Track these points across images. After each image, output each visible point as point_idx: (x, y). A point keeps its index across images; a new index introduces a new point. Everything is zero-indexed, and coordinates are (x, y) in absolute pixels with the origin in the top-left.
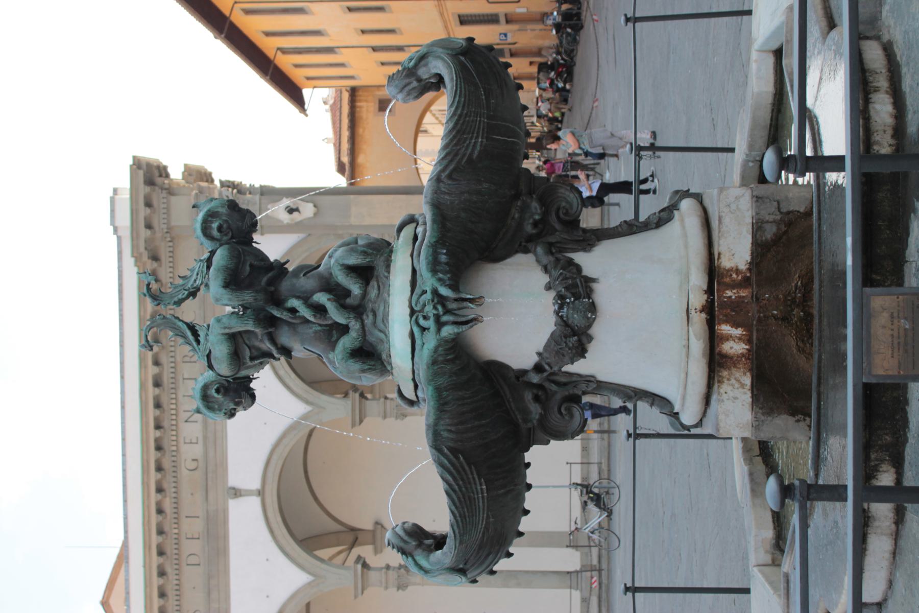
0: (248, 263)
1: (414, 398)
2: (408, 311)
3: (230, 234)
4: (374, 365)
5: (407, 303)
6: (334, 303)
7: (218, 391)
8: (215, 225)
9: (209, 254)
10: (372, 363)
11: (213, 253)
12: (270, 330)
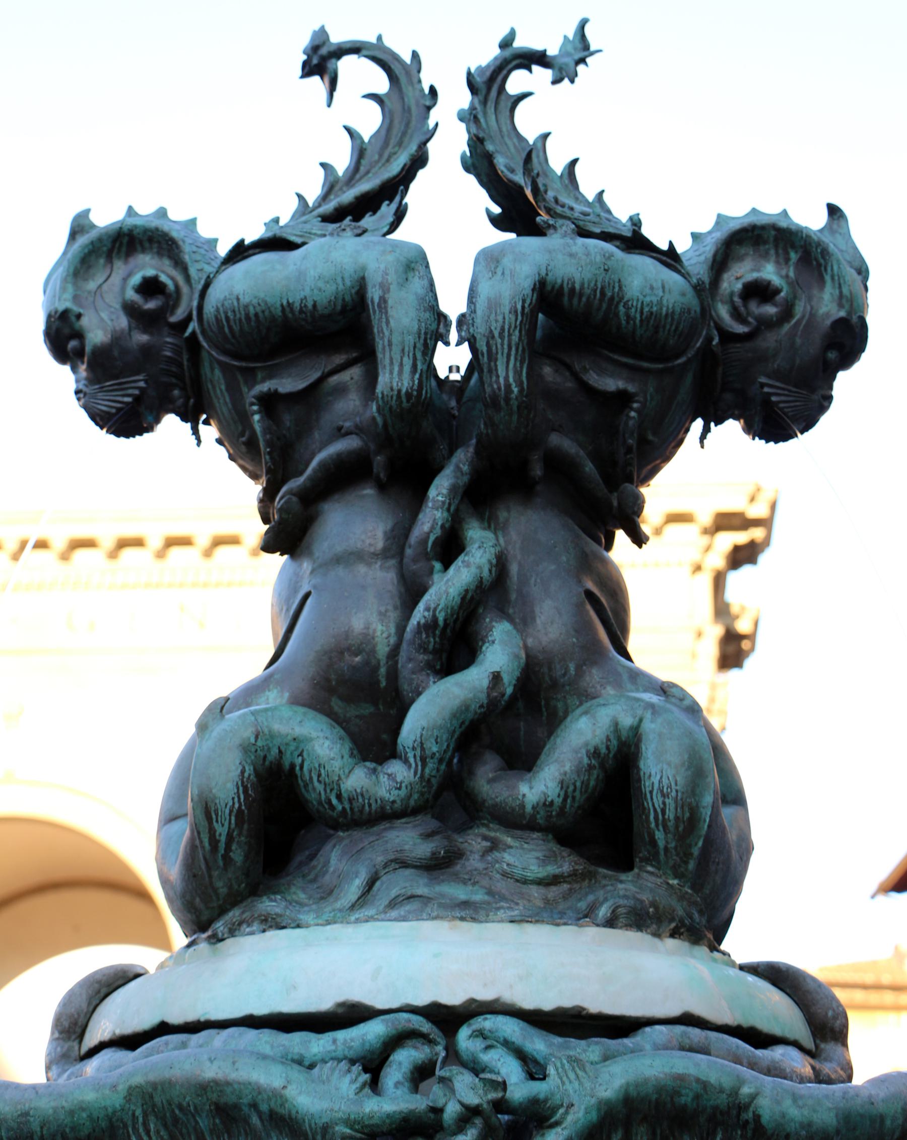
0: (631, 388)
1: (93, 1037)
2: (453, 997)
3: (740, 329)
4: (226, 858)
5: (485, 995)
6: (483, 698)
7: (150, 287)
8: (770, 272)
9: (664, 247)
10: (237, 855)
11: (670, 257)
12: (379, 460)
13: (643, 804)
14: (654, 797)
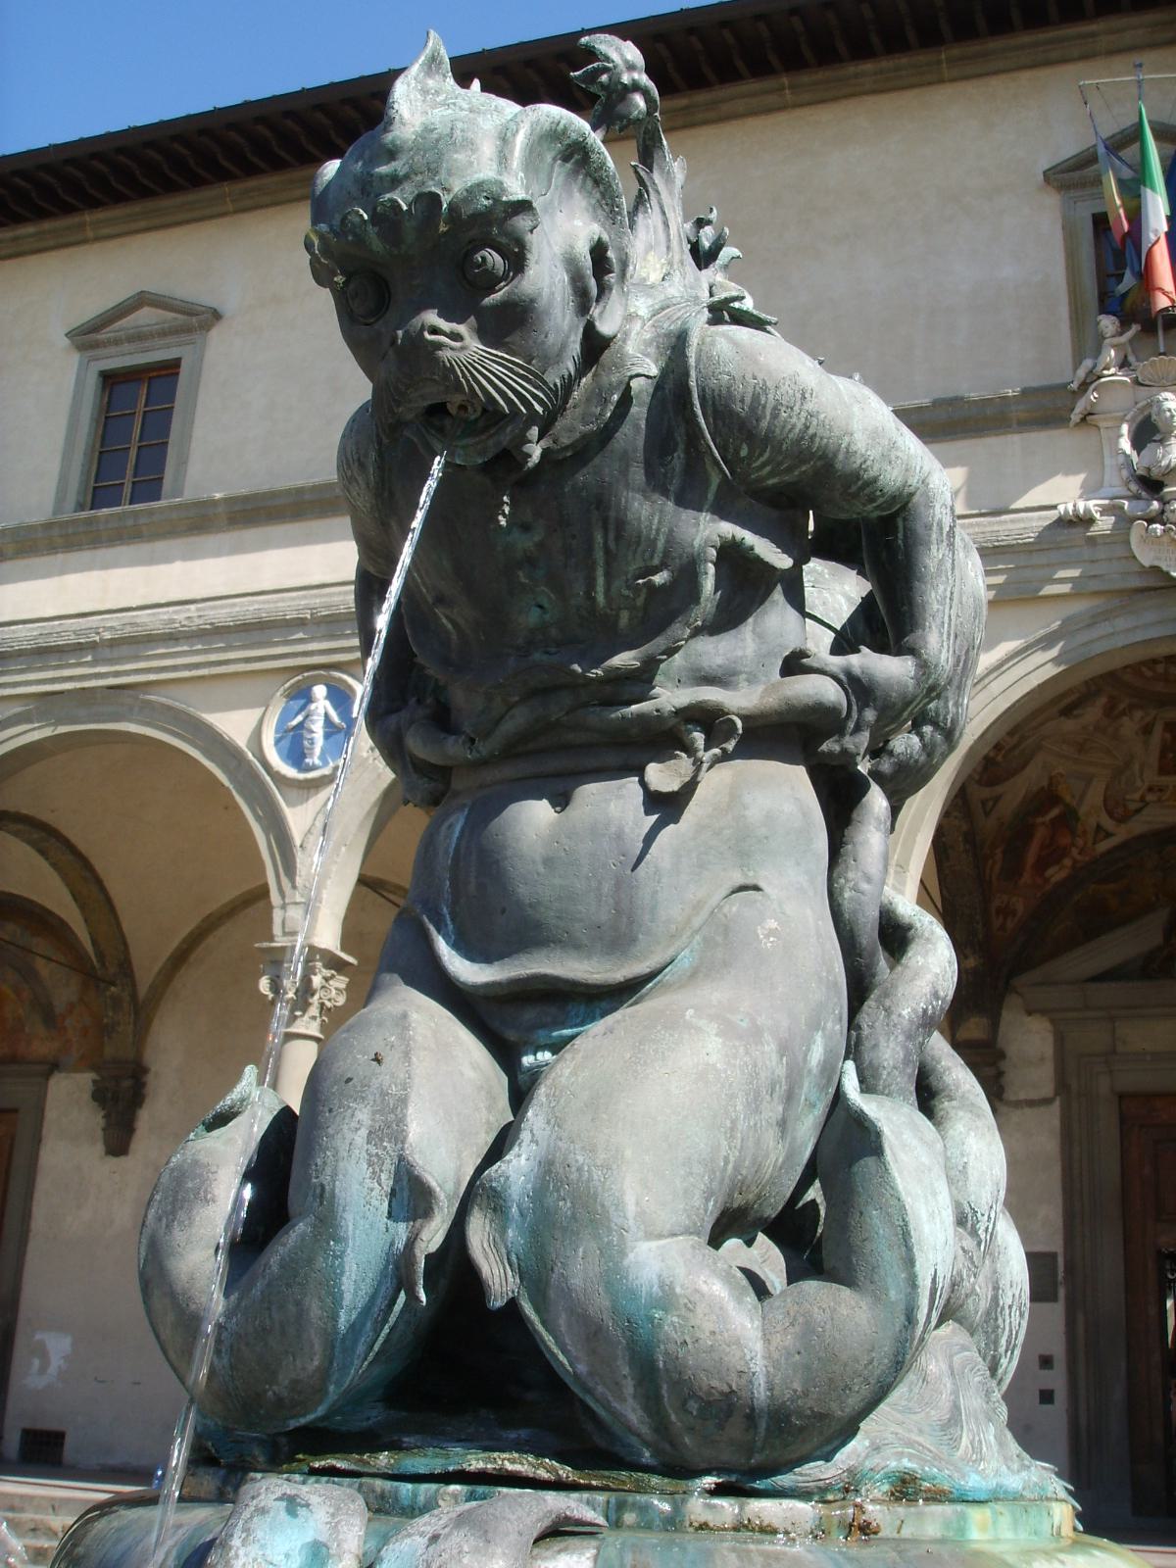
13: (996, 1319)
14: (1012, 1314)
